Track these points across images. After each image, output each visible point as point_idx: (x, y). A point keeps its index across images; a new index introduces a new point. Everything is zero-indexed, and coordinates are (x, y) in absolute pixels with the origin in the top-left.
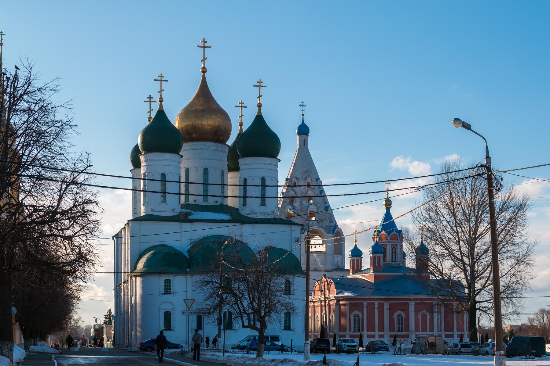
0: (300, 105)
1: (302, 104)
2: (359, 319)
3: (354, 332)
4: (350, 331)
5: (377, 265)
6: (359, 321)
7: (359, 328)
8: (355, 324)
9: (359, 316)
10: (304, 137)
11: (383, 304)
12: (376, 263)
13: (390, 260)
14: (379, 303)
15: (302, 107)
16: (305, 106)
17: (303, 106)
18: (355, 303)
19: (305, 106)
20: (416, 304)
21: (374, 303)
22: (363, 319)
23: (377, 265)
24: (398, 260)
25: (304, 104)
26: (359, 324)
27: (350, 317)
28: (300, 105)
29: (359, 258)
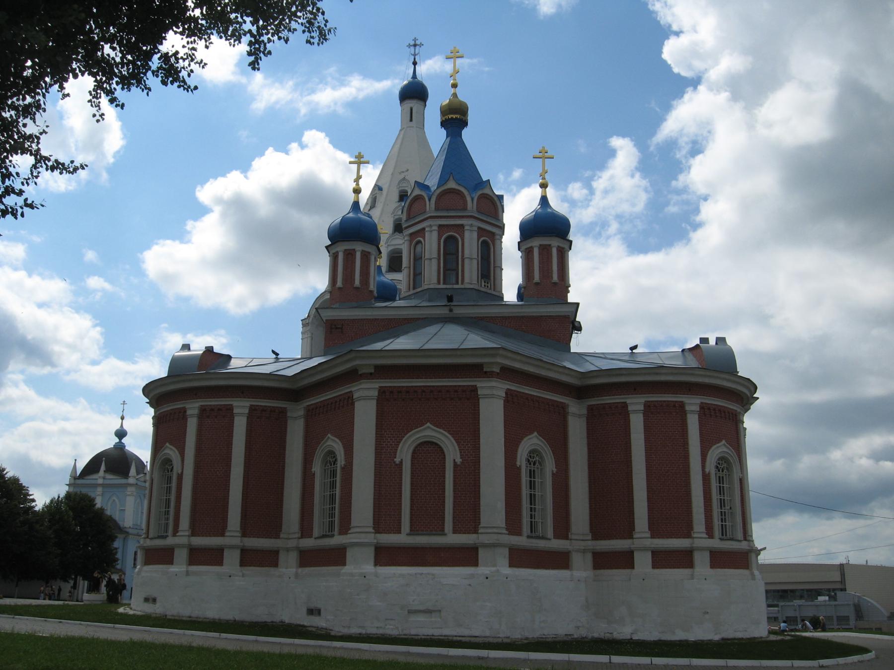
0: (409, 46)
1: (412, 43)
10: (414, 104)
11: (280, 417)
13: (435, 280)
14: (252, 409)
15: (412, 48)
16: (421, 45)
17: (415, 45)
19: (421, 45)
20: (384, 397)
21: (230, 409)
22: (180, 477)
24: (467, 280)
25: (418, 42)
28: (409, 46)
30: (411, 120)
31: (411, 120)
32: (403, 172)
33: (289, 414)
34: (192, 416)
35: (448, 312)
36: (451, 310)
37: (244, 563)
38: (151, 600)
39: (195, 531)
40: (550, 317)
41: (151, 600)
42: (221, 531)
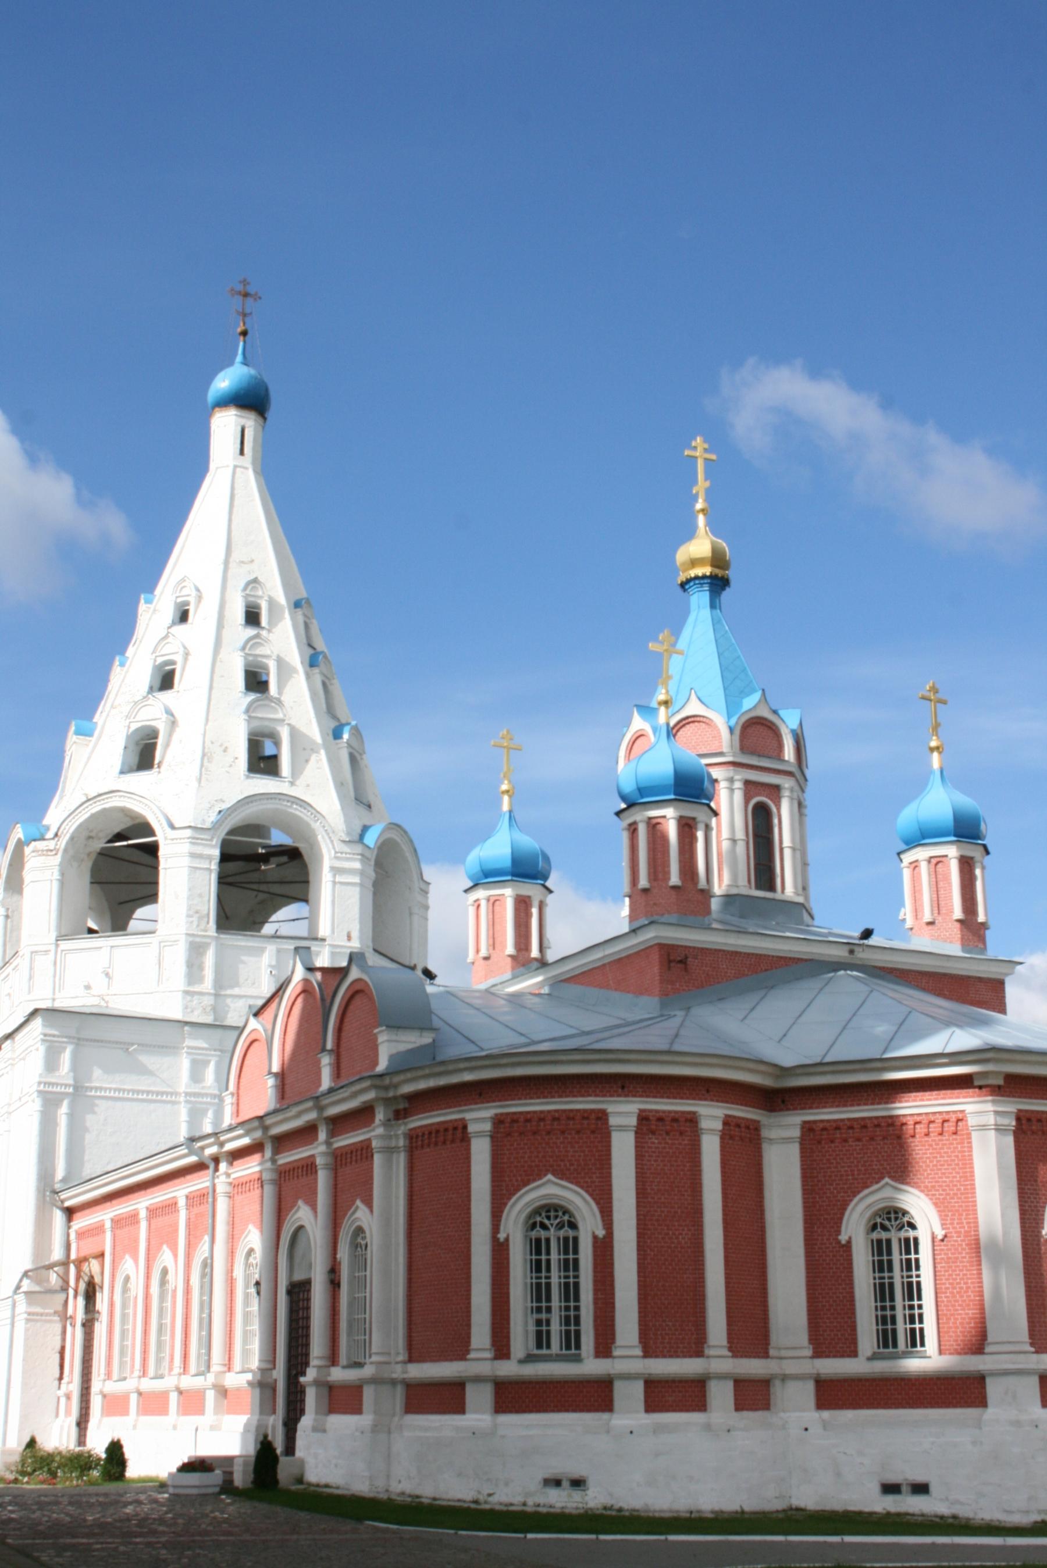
0: (233, 292)
1: (240, 287)
2: (570, 1245)
3: (529, 1359)
4: (501, 1348)
5: (675, 879)
6: (571, 1266)
7: (571, 1319)
8: (540, 1293)
9: (573, 1226)
12: (666, 864)
14: (728, 1121)
16: (257, 297)
18: (541, 1117)
19: (257, 297)
21: (692, 1120)
22: (604, 1248)
23: (675, 879)
25: (251, 289)
26: (571, 1292)
27: (496, 1227)
28: (233, 292)
29: (530, 889)
30: (242, 452)
31: (242, 452)
32: (243, 562)
33: (765, 1133)
34: (622, 1128)
35: (846, 954)
36: (852, 952)
37: (653, 1404)
38: (565, 1484)
39: (650, 1348)
40: (980, 980)
41: (565, 1484)
42: (697, 1347)
